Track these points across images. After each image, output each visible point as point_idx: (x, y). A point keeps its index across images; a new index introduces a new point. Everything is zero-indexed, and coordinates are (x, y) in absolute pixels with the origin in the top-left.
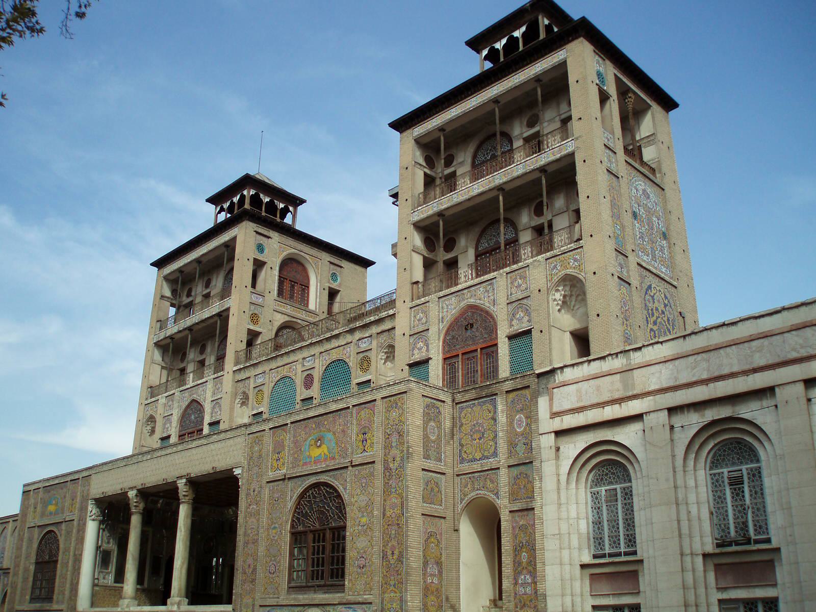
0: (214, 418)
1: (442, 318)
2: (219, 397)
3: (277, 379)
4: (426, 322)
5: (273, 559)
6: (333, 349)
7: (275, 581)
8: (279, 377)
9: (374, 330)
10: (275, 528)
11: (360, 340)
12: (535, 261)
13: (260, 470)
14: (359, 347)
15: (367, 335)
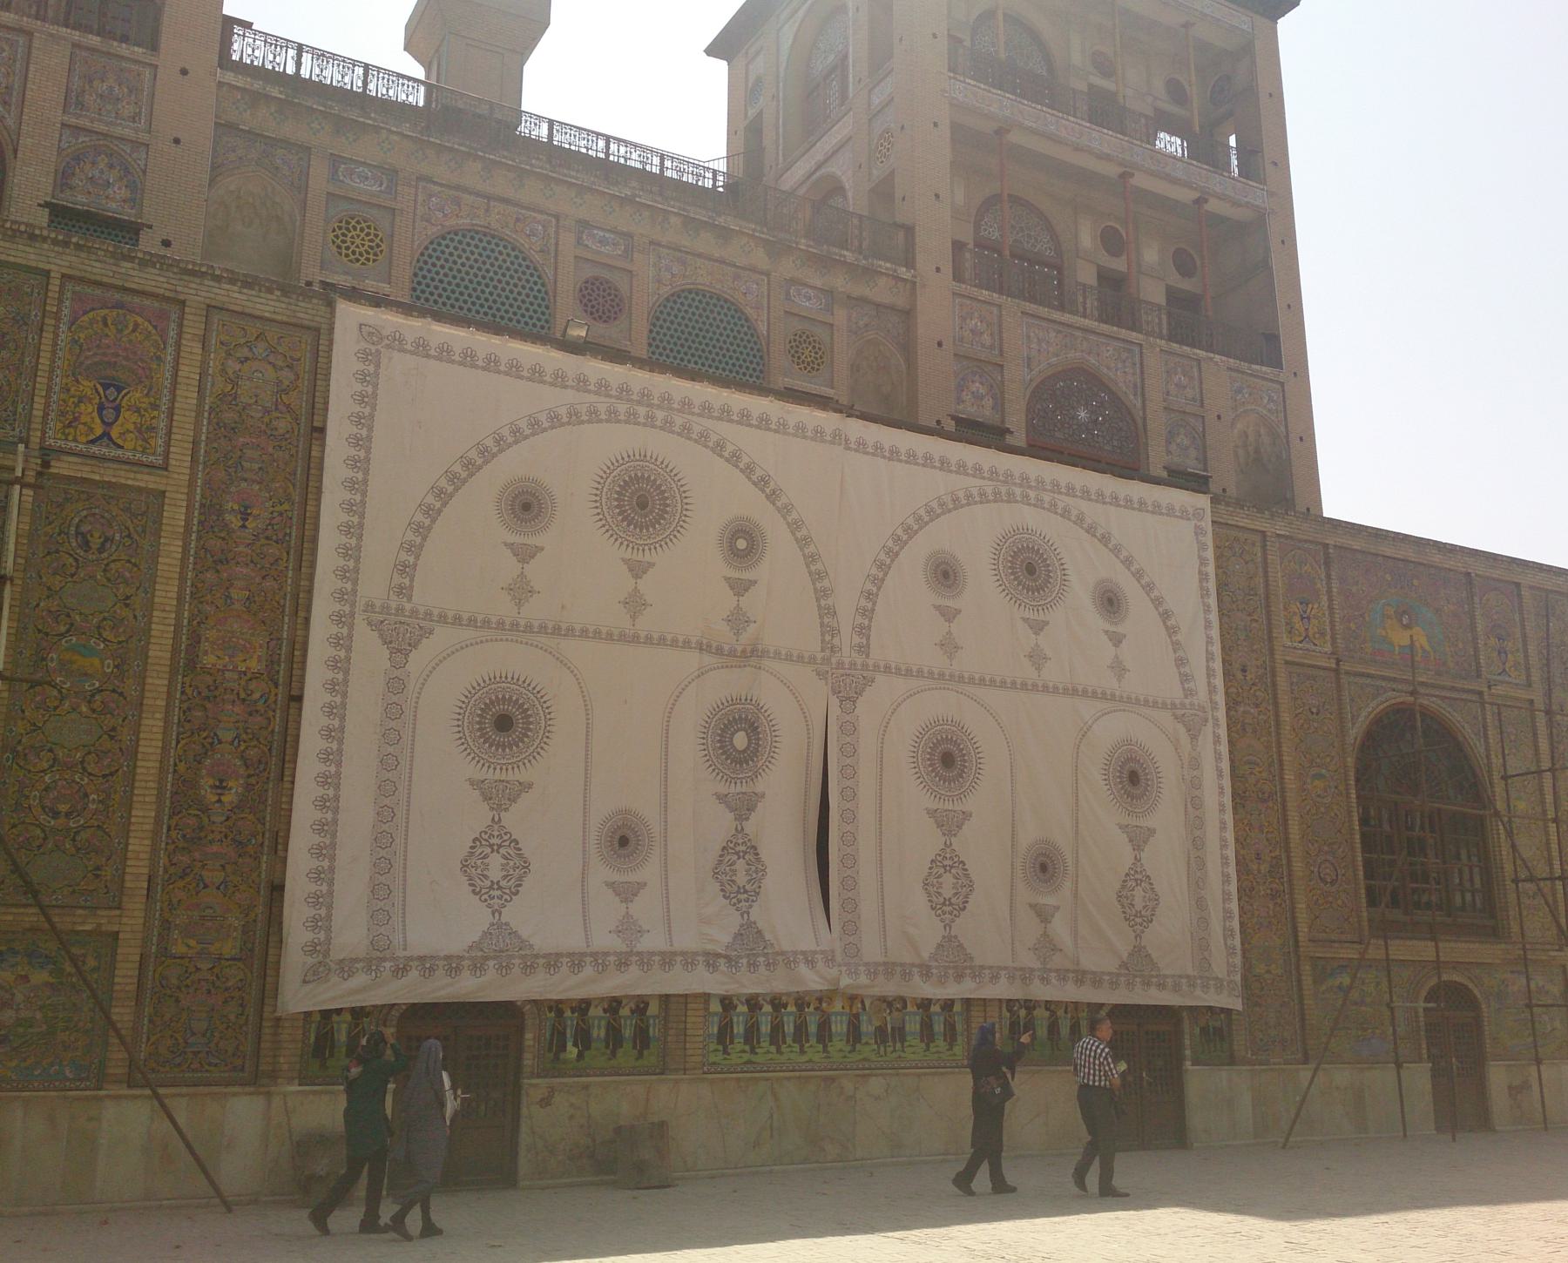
0: (81, 198)
1: (1029, 359)
2: (128, 133)
3: (452, 222)
4: (992, 347)
5: (1326, 848)
6: (700, 255)
7: (1340, 902)
8: (464, 222)
9: (840, 282)
10: (1319, 776)
11: (793, 281)
12: (1211, 359)
13: (1254, 625)
14: (788, 293)
15: (819, 283)
